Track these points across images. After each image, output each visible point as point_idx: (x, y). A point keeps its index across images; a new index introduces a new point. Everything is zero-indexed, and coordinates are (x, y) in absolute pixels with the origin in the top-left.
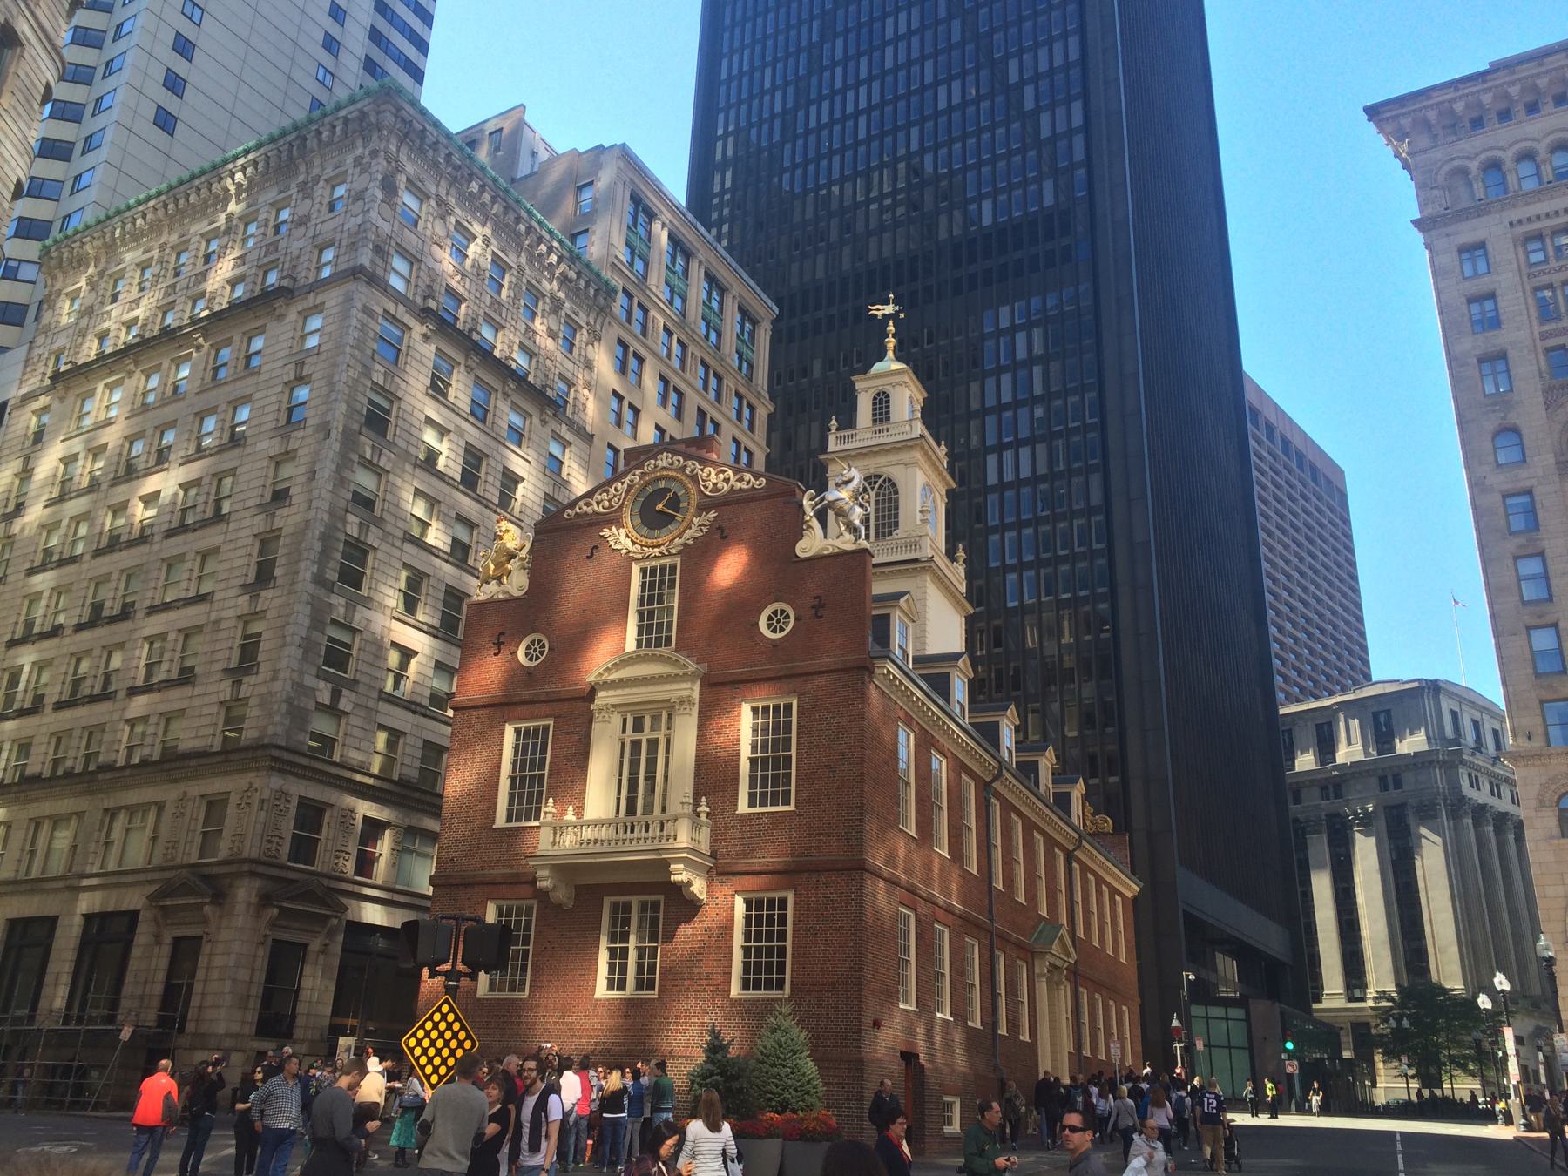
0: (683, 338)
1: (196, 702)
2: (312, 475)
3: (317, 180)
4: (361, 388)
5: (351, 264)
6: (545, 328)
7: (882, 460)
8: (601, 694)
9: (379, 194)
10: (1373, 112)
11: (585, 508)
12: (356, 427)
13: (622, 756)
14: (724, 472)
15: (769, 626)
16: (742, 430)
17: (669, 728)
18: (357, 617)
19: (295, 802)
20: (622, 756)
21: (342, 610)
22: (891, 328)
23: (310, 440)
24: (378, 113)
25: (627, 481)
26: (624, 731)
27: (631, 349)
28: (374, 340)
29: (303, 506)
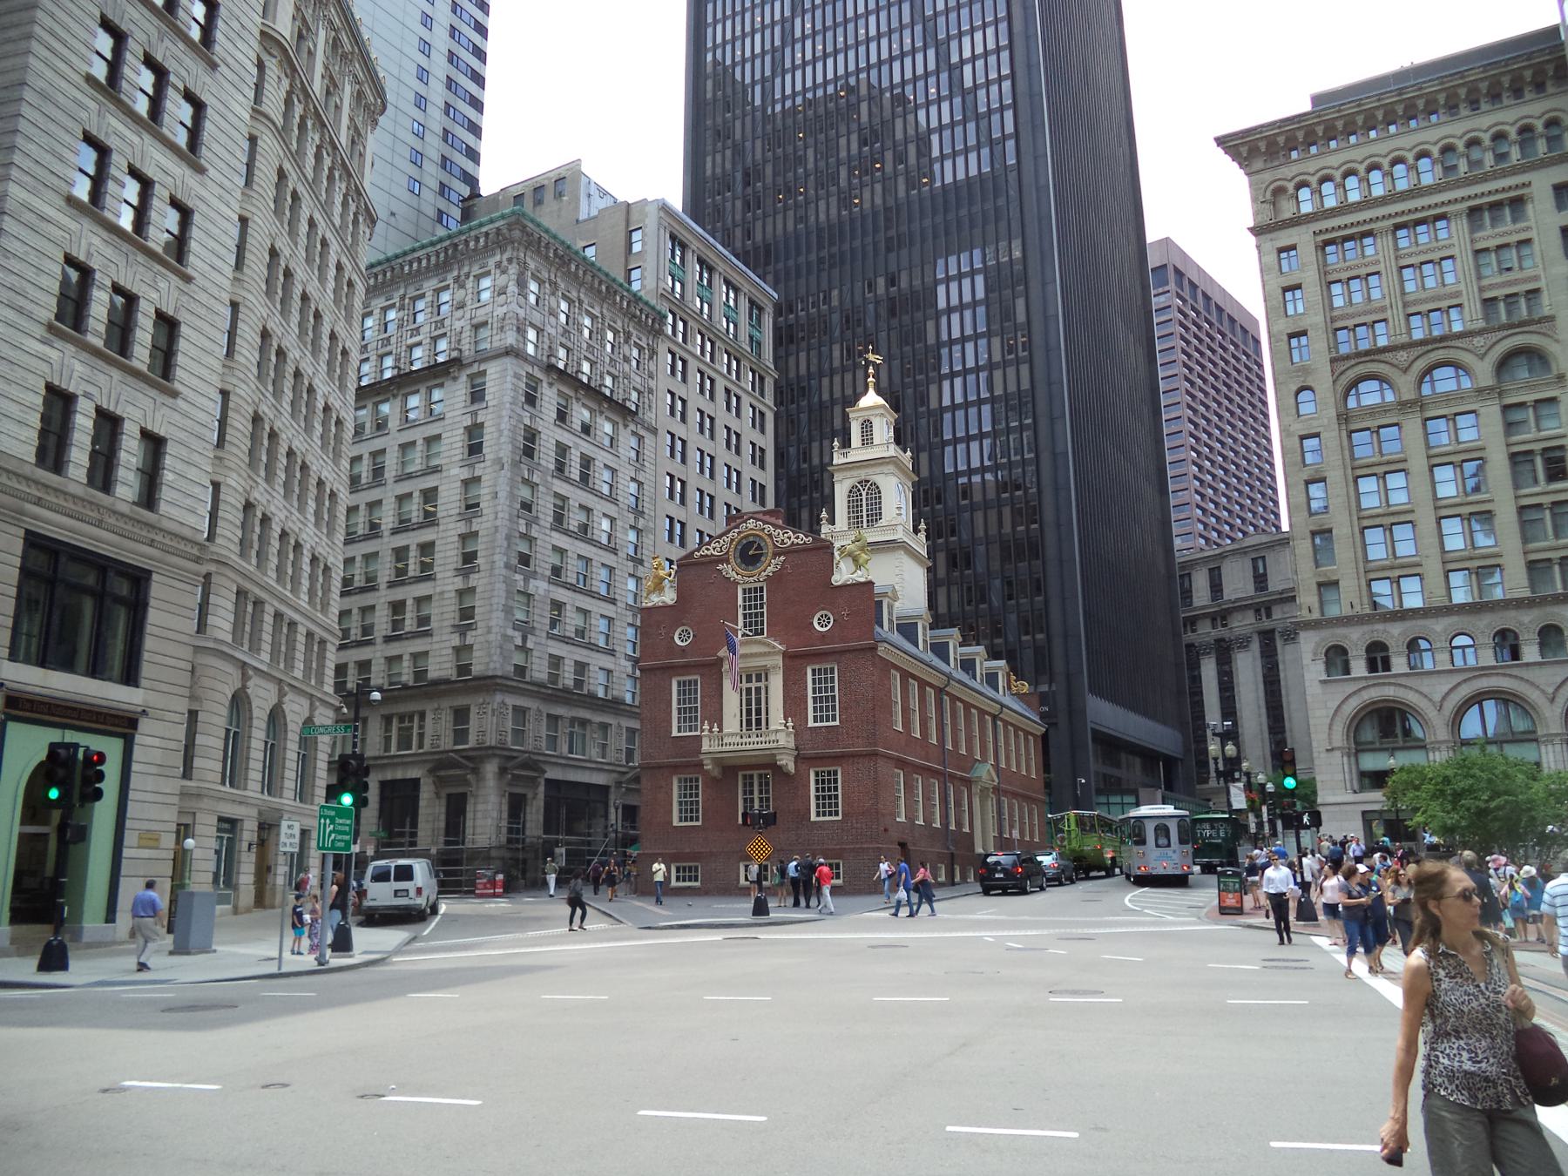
0: (712, 336)
1: (436, 646)
2: (495, 495)
3: (467, 276)
7: (870, 471)
9: (516, 291)
10: (1221, 141)
16: (755, 398)
18: (531, 586)
19: (510, 708)
21: (522, 583)
22: (871, 370)
23: (487, 471)
29: (492, 517)
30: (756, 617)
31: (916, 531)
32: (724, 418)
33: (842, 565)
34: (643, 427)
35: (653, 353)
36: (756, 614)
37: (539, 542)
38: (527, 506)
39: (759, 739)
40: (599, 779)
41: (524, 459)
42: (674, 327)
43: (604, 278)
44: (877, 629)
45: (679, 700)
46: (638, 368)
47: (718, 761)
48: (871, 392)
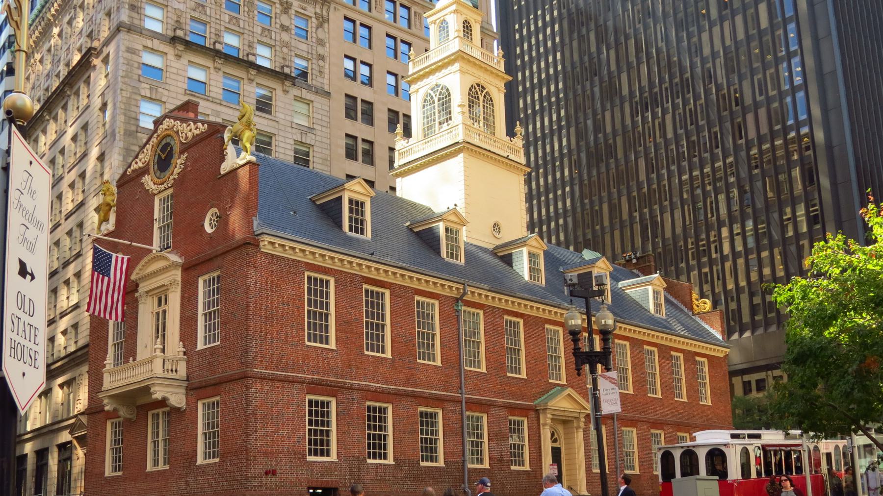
4: (133, 102)
6: (278, 26)
8: (141, 285)
15: (210, 224)
25: (151, 143)
27: (358, 23)
28: (139, 68)
35: (323, 21)
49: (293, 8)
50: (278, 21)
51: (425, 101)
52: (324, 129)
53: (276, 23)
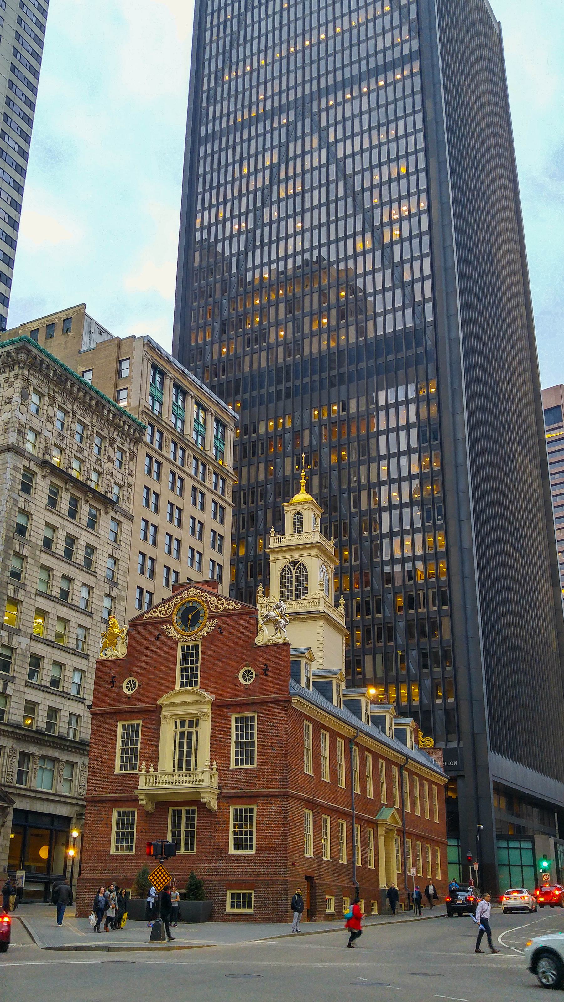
4: (13, 513)
5: (6, 441)
7: (299, 553)
9: (20, 401)
11: (153, 614)
12: (11, 535)
13: (175, 739)
14: (221, 600)
15: (243, 678)
17: (197, 726)
20: (175, 739)
21: (7, 638)
24: (18, 354)
26: (176, 727)
27: (154, 459)
30: (192, 671)
31: (337, 605)
32: (189, 510)
33: (264, 628)
34: (122, 514)
35: (134, 455)
36: (192, 668)
37: (24, 605)
38: (16, 575)
39: (188, 779)
40: (62, 811)
41: (19, 537)
42: (152, 437)
43: (94, 395)
44: (292, 683)
45: (123, 741)
46: (120, 468)
47: (150, 797)
48: (303, 491)
49: (116, 443)
50: (107, 453)
51: (283, 570)
52: (127, 547)
53: (105, 455)
